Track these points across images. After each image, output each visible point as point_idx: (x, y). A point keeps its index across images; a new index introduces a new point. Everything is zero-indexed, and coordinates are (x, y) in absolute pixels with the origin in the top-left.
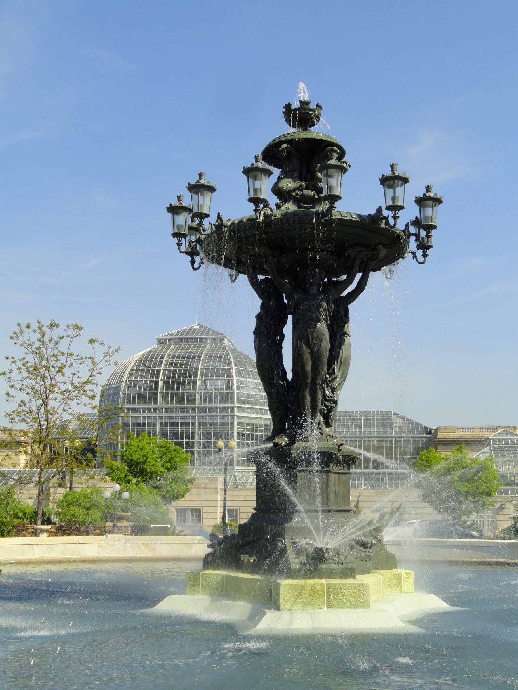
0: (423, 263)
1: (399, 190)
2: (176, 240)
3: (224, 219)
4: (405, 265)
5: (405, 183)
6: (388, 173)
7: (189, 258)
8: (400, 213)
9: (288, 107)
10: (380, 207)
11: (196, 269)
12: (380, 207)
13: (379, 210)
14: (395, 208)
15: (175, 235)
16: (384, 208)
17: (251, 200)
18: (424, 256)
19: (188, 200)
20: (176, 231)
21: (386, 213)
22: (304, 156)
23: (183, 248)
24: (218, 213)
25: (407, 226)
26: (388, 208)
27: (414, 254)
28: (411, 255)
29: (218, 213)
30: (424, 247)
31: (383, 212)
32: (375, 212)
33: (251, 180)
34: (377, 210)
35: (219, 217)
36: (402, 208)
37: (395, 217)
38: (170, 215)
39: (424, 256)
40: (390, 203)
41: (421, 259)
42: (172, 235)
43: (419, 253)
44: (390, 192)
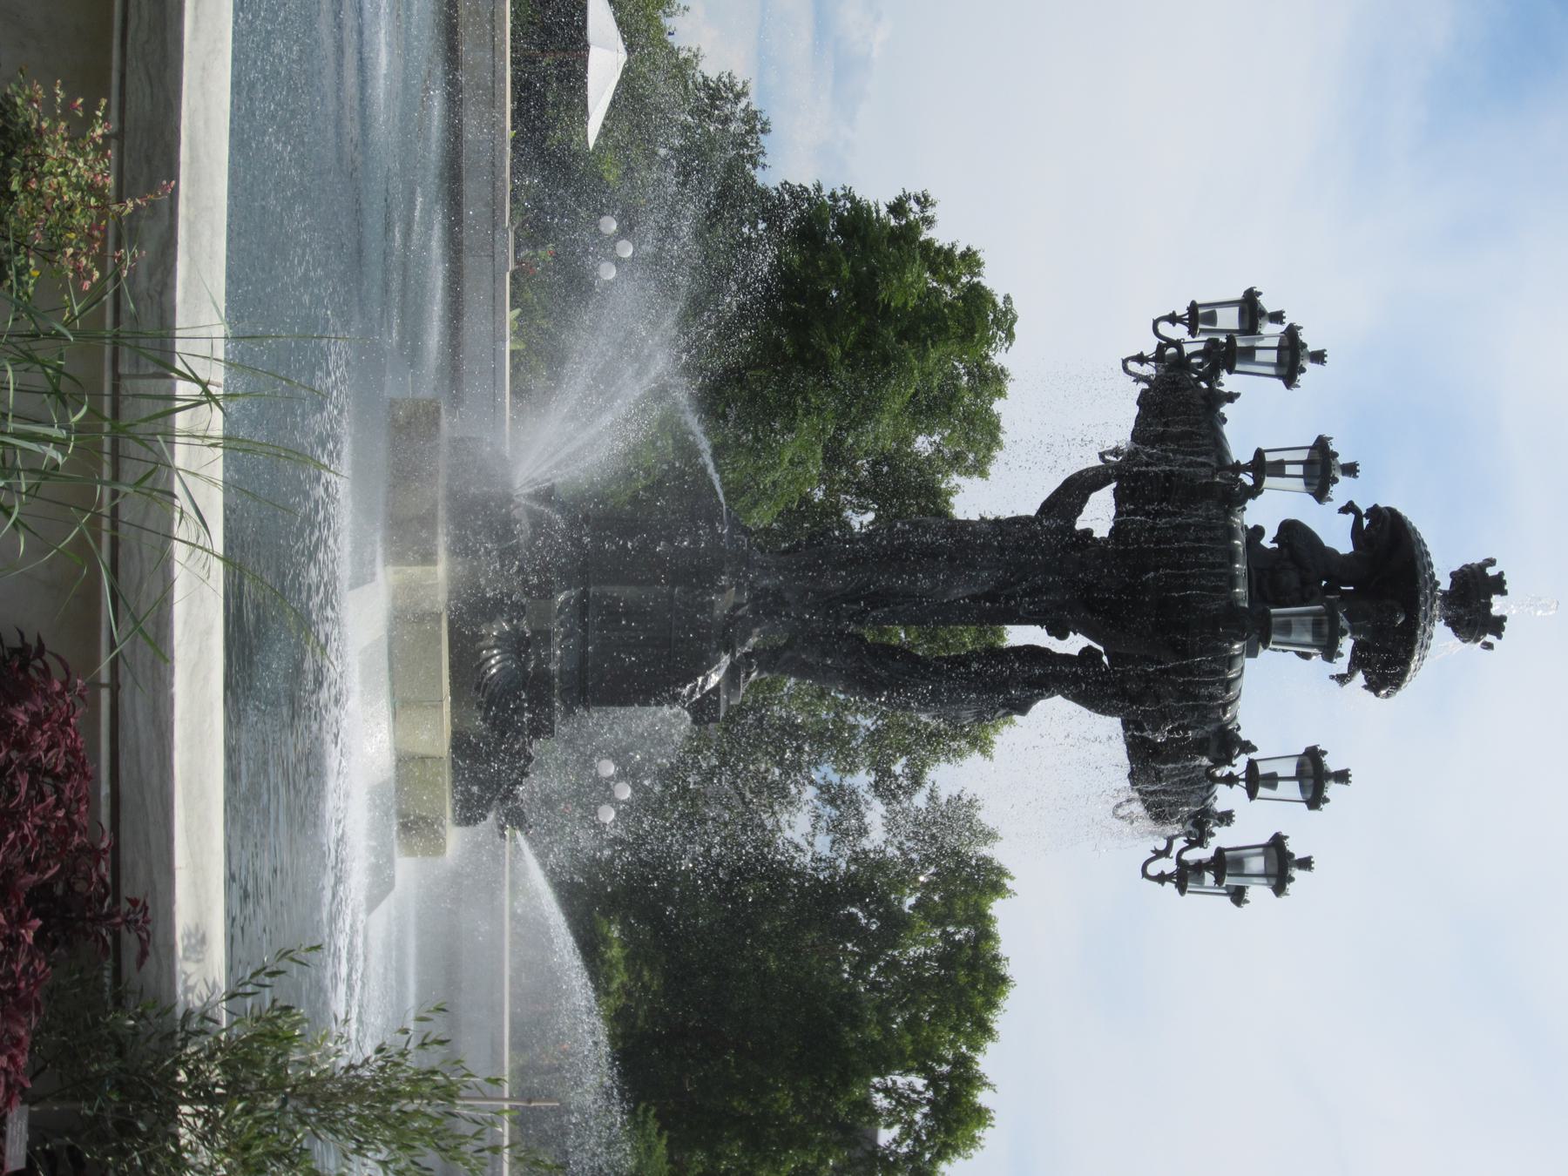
0: (1145, 874)
1: (1291, 789)
2: (1182, 311)
3: (1226, 409)
4: (1144, 839)
6: (1332, 764)
7: (1150, 348)
8: (1239, 791)
9: (1491, 562)
10: (1254, 749)
11: (1125, 369)
12: (1254, 749)
13: (1248, 747)
15: (1193, 308)
16: (1253, 756)
17: (1259, 454)
18: (1162, 878)
19: (1271, 332)
20: (1201, 311)
21: (1240, 765)
22: (1383, 598)
23: (1166, 329)
24: (1238, 395)
26: (1252, 765)
27: (1165, 853)
28: (1162, 845)
29: (1238, 395)
30: (1185, 877)
32: (1244, 738)
33: (1303, 455)
34: (1248, 743)
35: (1231, 397)
36: (1252, 795)
37: (1231, 780)
38: (1239, 296)
39: (1162, 878)
40: (1263, 769)
41: (1154, 869)
42: (1193, 303)
43: (1168, 865)
44: (1289, 769)
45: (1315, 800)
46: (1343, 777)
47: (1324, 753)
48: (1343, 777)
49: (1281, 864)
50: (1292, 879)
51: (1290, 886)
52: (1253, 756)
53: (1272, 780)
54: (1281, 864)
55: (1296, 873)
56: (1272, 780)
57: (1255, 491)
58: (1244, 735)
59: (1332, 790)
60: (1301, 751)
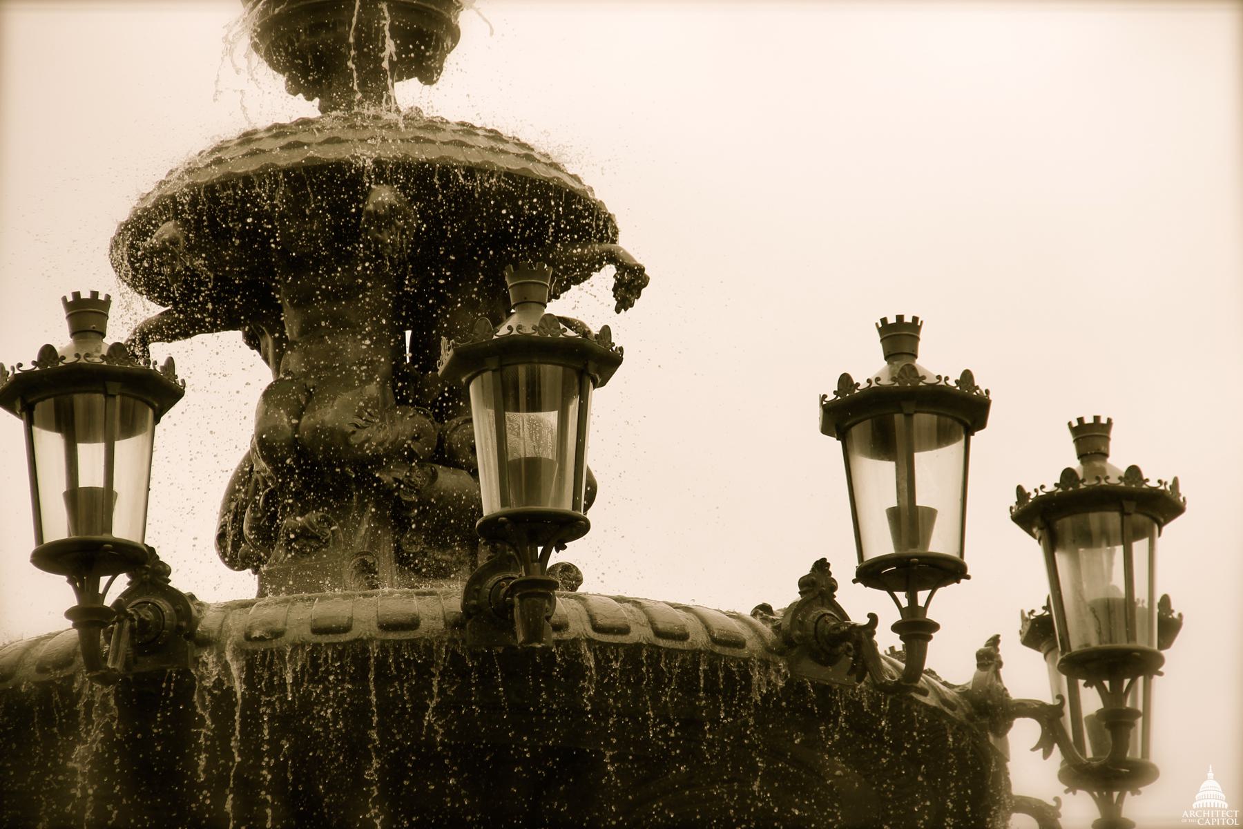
1: (934, 468)
5: (969, 431)
6: (870, 366)
8: (942, 604)
10: (822, 566)
12: (822, 566)
13: (818, 583)
14: (915, 568)
16: (844, 570)
17: (50, 557)
21: (858, 602)
25: (989, 658)
26: (870, 574)
31: (840, 597)
32: (794, 595)
34: (805, 584)
36: (950, 570)
37: (916, 629)
40: (881, 544)
44: (879, 477)
45: (962, 410)
46: (899, 337)
47: (845, 381)
48: (899, 337)
49: (1096, 506)
50: (1134, 471)
51: (1153, 477)
52: (844, 570)
53: (909, 519)
54: (1096, 506)
55: (1118, 460)
56: (909, 519)
57: (143, 564)
58: (785, 596)
59: (936, 361)
60: (834, 445)
